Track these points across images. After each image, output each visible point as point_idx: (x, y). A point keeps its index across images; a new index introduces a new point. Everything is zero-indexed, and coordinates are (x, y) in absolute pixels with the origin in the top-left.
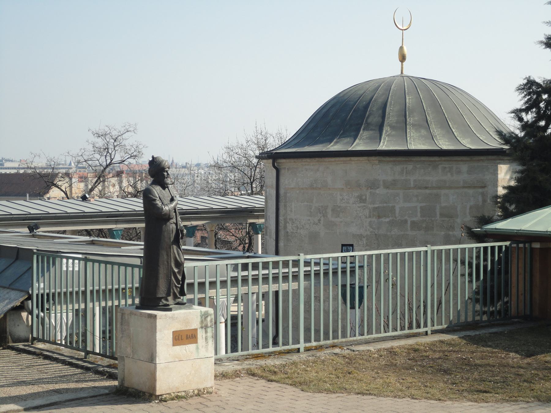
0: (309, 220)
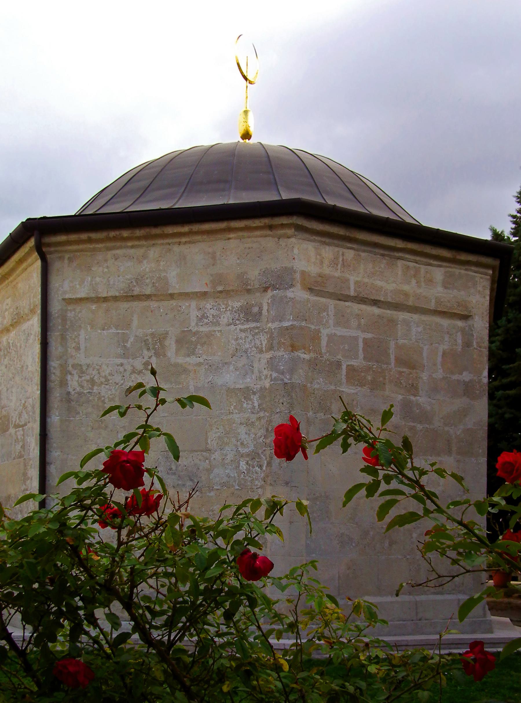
0: (122, 365)
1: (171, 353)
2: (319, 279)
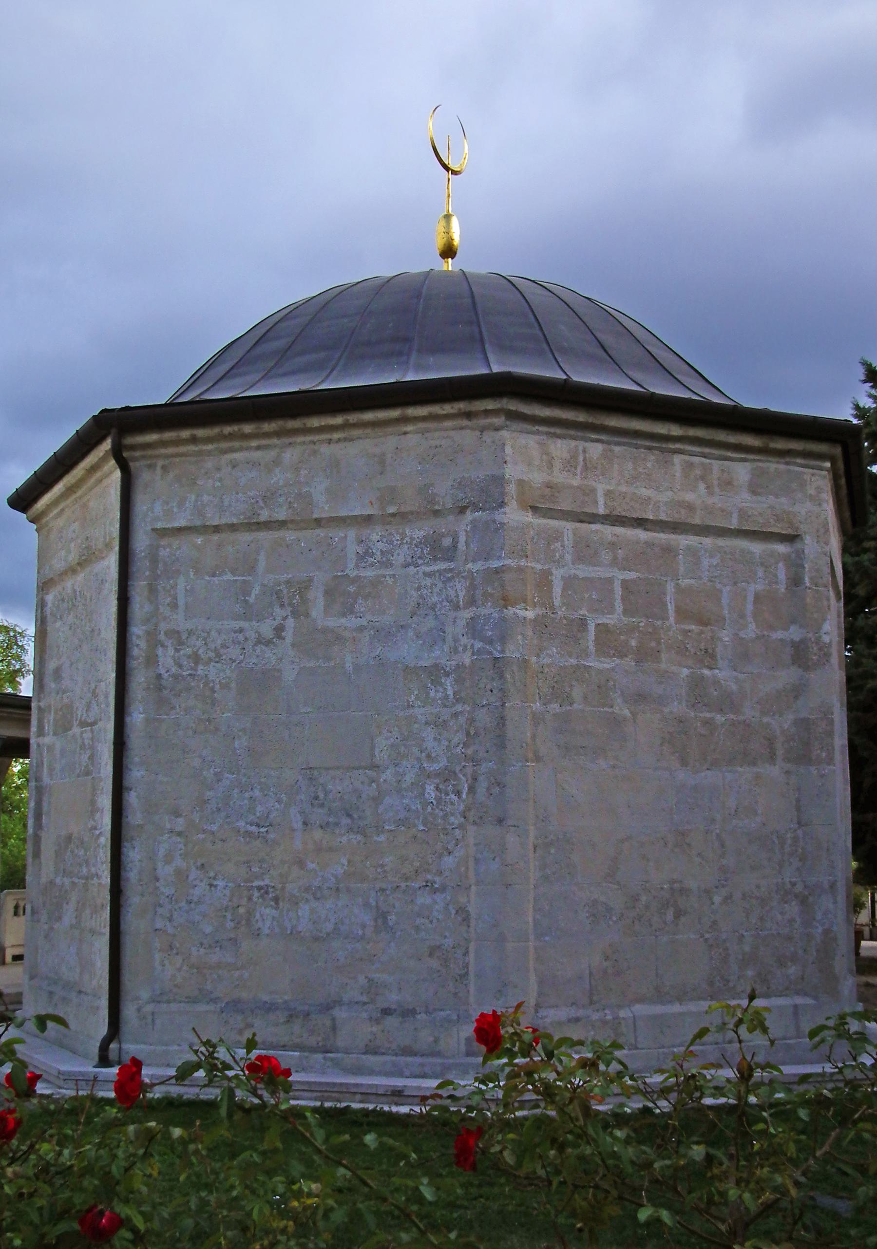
0: (241, 631)
1: (317, 611)
2: (547, 491)
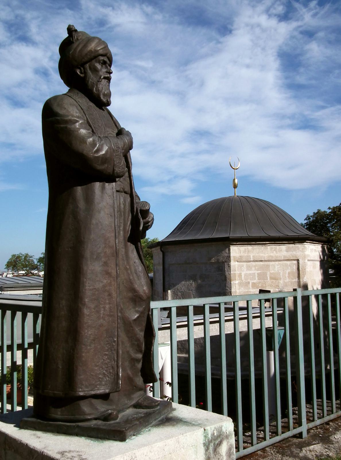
2: (240, 257)
